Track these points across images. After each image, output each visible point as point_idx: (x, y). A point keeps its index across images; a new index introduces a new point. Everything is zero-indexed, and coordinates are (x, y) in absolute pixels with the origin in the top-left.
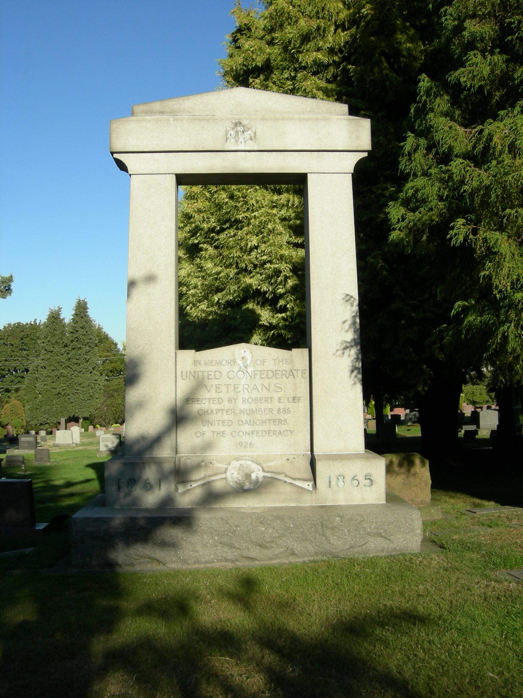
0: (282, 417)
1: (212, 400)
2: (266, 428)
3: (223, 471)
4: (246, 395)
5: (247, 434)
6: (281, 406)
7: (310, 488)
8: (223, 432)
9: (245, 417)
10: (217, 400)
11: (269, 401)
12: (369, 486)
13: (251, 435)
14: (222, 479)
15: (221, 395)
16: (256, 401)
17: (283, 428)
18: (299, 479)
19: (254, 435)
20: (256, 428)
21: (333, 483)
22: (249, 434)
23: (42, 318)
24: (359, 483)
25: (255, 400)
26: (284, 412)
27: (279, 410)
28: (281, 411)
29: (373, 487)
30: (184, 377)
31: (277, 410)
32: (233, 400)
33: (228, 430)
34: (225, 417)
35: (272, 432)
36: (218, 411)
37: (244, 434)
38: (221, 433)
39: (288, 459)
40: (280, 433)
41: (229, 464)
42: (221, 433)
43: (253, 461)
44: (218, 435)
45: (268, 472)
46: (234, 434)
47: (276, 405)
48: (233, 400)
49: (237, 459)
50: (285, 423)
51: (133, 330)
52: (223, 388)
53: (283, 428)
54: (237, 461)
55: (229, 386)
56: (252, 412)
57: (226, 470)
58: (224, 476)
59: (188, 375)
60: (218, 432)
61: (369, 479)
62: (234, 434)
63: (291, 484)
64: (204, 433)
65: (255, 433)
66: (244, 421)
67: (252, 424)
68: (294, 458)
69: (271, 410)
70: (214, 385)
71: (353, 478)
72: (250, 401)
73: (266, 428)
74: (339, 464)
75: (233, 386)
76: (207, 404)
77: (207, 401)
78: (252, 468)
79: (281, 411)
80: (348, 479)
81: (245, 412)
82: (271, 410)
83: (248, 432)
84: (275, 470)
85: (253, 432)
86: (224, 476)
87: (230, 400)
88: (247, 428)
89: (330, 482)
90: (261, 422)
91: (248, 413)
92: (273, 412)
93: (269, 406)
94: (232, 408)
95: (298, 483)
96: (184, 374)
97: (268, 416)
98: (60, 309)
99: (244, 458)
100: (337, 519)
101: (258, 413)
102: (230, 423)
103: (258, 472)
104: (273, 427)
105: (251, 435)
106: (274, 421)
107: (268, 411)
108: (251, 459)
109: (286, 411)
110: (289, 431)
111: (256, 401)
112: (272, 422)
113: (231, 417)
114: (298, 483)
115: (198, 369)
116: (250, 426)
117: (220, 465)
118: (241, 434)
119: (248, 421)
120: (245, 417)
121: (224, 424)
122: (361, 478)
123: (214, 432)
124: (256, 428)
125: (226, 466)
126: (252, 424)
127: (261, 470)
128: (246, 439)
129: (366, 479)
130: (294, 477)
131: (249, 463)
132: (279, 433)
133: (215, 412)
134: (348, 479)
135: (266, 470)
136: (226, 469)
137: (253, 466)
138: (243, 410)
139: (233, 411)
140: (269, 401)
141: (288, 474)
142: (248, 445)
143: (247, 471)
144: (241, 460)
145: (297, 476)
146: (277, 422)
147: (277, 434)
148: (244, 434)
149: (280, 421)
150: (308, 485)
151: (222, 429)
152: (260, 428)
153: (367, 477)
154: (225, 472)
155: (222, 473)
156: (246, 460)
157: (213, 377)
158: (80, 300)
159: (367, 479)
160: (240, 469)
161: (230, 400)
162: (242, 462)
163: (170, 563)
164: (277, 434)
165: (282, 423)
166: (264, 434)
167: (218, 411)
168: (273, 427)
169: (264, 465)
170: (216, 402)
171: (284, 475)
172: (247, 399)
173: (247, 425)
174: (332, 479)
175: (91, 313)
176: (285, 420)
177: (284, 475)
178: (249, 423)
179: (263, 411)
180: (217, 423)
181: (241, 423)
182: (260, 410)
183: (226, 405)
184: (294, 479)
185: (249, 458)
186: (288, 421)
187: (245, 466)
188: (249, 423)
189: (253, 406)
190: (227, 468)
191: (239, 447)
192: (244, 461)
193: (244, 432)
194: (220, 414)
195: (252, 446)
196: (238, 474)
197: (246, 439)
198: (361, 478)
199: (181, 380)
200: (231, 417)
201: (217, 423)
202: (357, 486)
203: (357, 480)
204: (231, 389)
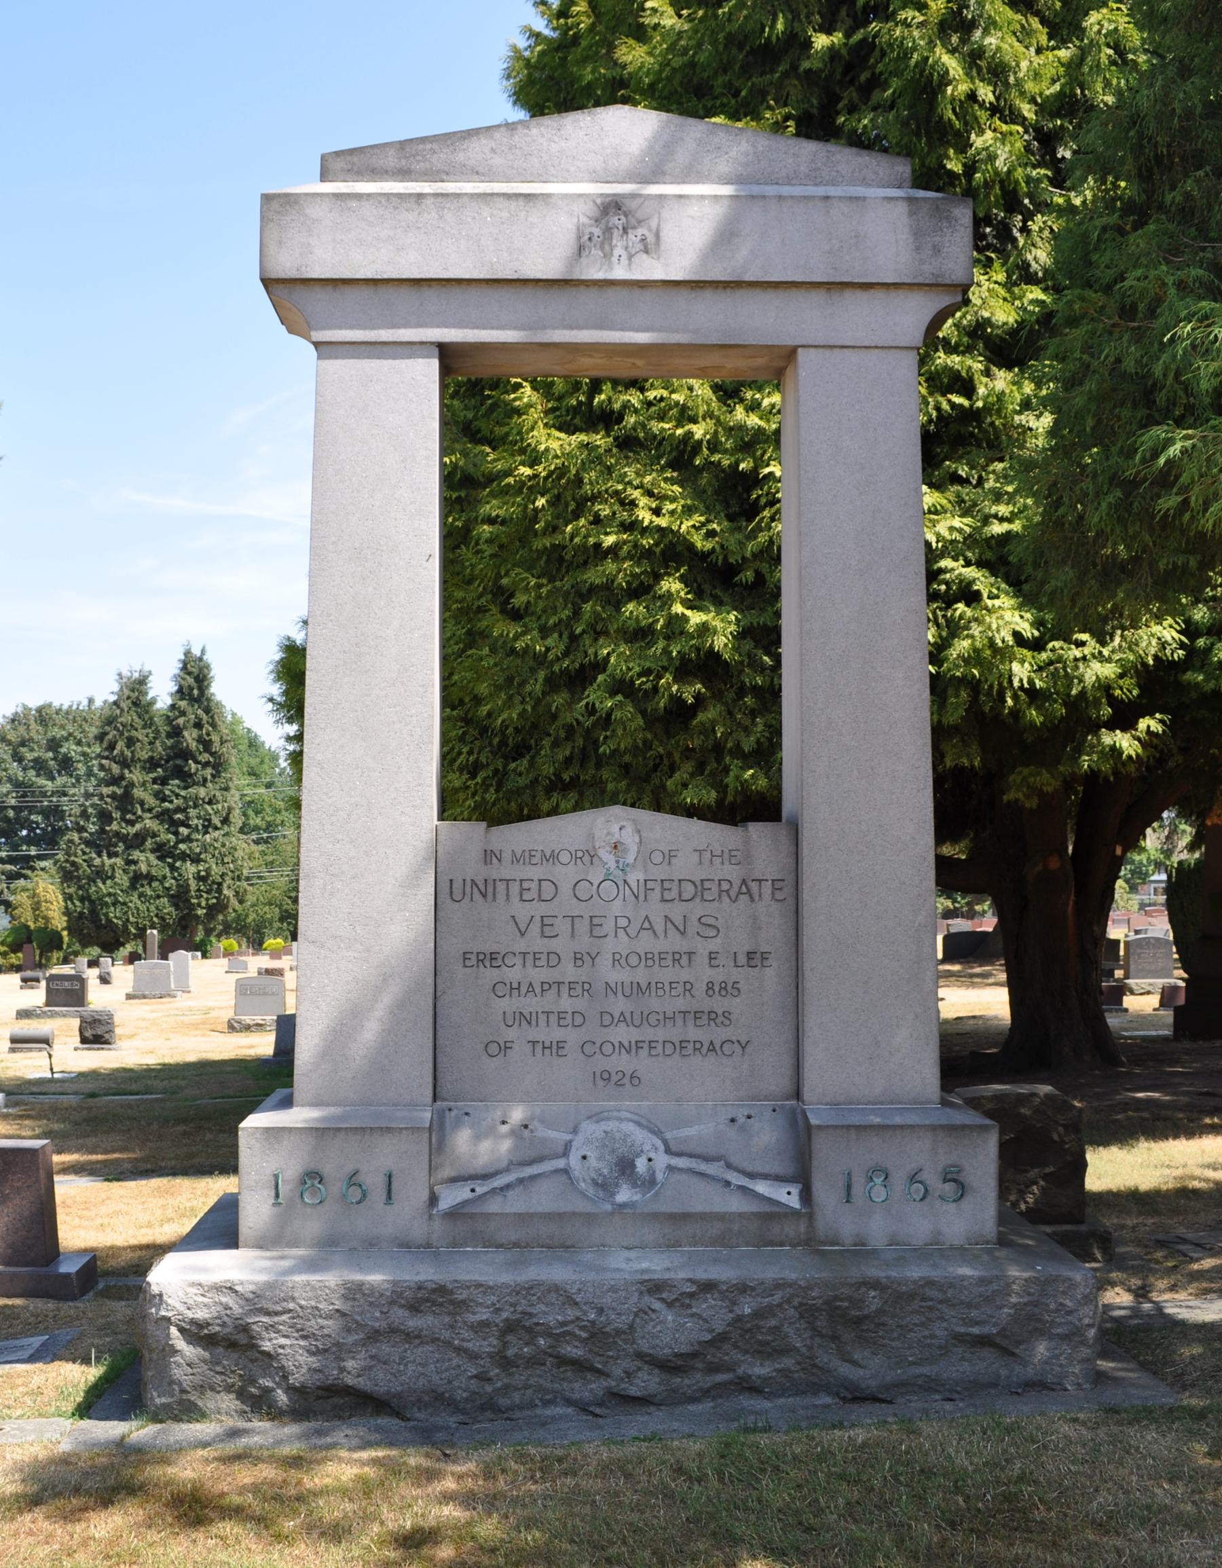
0: (719, 1004)
1: (531, 956)
2: (675, 1033)
3: (561, 1149)
4: (622, 944)
5: (623, 1050)
6: (718, 976)
7: (794, 1202)
8: (560, 1045)
9: (619, 1005)
10: (544, 957)
11: (684, 961)
12: (954, 1201)
13: (634, 1051)
14: (557, 1171)
15: (555, 945)
16: (650, 963)
17: (719, 1034)
18: (765, 1177)
19: (644, 1053)
20: (648, 1033)
21: (858, 1189)
22: (628, 1052)
23: (105, 691)
24: (926, 1190)
25: (647, 958)
26: (723, 993)
27: (710, 986)
28: (717, 988)
29: (965, 1204)
30: (457, 896)
31: (705, 988)
32: (586, 957)
33: (573, 1037)
34: (566, 1003)
35: (691, 1046)
36: (546, 987)
37: (617, 1051)
38: (555, 1047)
39: (733, 1120)
40: (712, 1048)
41: (575, 1131)
42: (555, 1047)
43: (638, 1124)
44: (547, 1052)
45: (679, 1154)
46: (589, 1049)
47: (703, 973)
48: (586, 957)
49: (597, 1117)
50: (727, 1022)
51: (322, 768)
52: (562, 926)
53: (719, 1034)
54: (597, 1122)
55: (576, 920)
56: (639, 989)
57: (568, 1146)
58: (560, 1163)
59: (468, 889)
60: (547, 1044)
61: (955, 1181)
62: (589, 1049)
63: (742, 1189)
64: (508, 1045)
65: (646, 1046)
66: (616, 1016)
67: (637, 1023)
68: (749, 1117)
69: (688, 986)
70: (538, 919)
71: (913, 1178)
72: (634, 960)
73: (675, 1033)
74: (875, 1139)
75: (587, 921)
76: (519, 967)
77: (518, 961)
78: (638, 1143)
79: (717, 988)
80: (899, 1178)
81: (619, 988)
82: (688, 987)
83: (626, 1044)
84: (699, 1150)
85: (638, 1045)
86: (560, 1163)
87: (577, 958)
88: (622, 1034)
89: (849, 1187)
90: (661, 1017)
91: (628, 992)
92: (694, 992)
93: (685, 975)
94: (584, 979)
95: (761, 1187)
96: (457, 886)
97: (681, 1003)
98: (150, 673)
99: (615, 1114)
100: (873, 1293)
101: (653, 994)
102: (579, 1020)
103: (652, 1155)
104: (693, 1033)
105: (634, 1051)
106: (697, 1015)
107: (680, 989)
108: (636, 1118)
109: (728, 989)
110: (736, 1044)
111: (650, 963)
112: (690, 1017)
113: (581, 1004)
114: (761, 1187)
115: (494, 875)
116: (632, 1028)
117: (552, 1134)
118: (607, 1049)
119: (628, 1016)
120: (619, 1005)
121: (562, 1022)
122: (931, 1177)
123: (534, 1043)
124: (648, 1033)
125: (569, 1137)
126: (637, 1023)
127: (662, 1148)
128: (623, 1062)
129: (945, 1181)
130: (749, 1169)
131: (629, 1127)
132: (709, 1050)
133: (538, 990)
134: (899, 1178)
135: (674, 1148)
136: (566, 1145)
137: (640, 1136)
138: (613, 986)
139: (587, 988)
140: (684, 961)
141: (733, 1160)
142: (626, 1080)
143: (623, 1150)
144: (608, 1119)
145: (758, 1167)
146: (705, 1017)
147: (704, 1050)
148: (617, 1051)
149: (712, 1016)
150: (789, 1193)
151: (557, 1034)
152: (660, 1034)
153: (949, 1176)
154: (566, 1153)
155: (556, 1156)
156: (620, 1119)
157: (536, 896)
158: (187, 653)
159: (949, 1180)
160: (605, 1146)
161: (577, 958)
162: (611, 1126)
163: (416, 1409)
164: (704, 1050)
165: (719, 1020)
166: (669, 1047)
167: (546, 987)
168: (693, 1033)
169: (668, 1136)
170: (543, 962)
171: (722, 1163)
172: (624, 955)
173: (623, 1024)
174: (854, 1179)
175: (219, 690)
176: (727, 1015)
177: (722, 1163)
178: (629, 1020)
179: (667, 988)
180: (542, 1018)
181: (607, 1019)
182: (660, 985)
183: (569, 971)
184: (752, 1176)
185: (629, 1115)
186: (733, 1017)
187: (617, 1135)
188: (629, 1020)
189: (641, 976)
190: (571, 1141)
191: (601, 1083)
192: (617, 1123)
193: (617, 1045)
194: (551, 995)
195: (636, 1081)
196: (600, 1158)
197: (623, 1062)
198: (931, 1177)
199: (449, 901)
200: (581, 1004)
201: (542, 1018)
202: (921, 1200)
203: (920, 1182)
204: (583, 927)
